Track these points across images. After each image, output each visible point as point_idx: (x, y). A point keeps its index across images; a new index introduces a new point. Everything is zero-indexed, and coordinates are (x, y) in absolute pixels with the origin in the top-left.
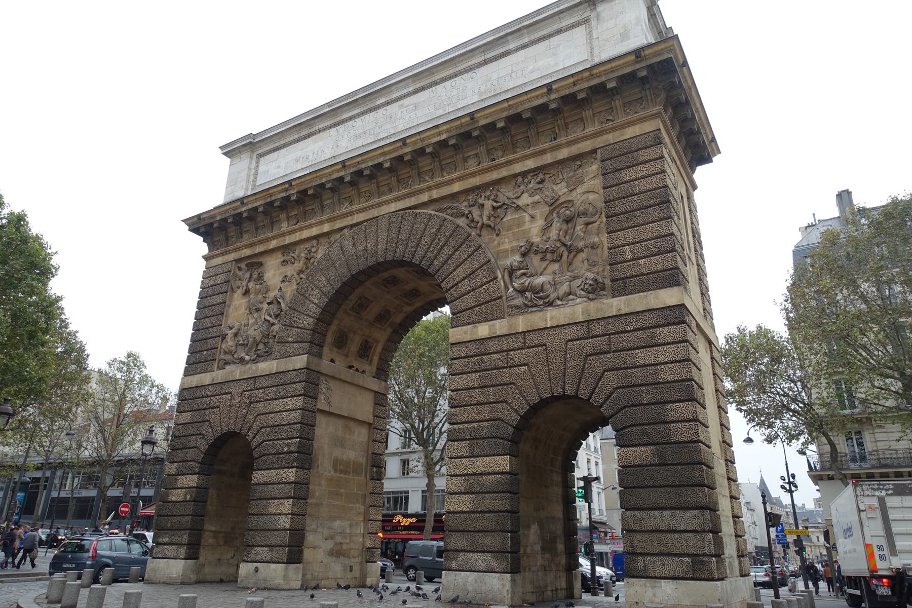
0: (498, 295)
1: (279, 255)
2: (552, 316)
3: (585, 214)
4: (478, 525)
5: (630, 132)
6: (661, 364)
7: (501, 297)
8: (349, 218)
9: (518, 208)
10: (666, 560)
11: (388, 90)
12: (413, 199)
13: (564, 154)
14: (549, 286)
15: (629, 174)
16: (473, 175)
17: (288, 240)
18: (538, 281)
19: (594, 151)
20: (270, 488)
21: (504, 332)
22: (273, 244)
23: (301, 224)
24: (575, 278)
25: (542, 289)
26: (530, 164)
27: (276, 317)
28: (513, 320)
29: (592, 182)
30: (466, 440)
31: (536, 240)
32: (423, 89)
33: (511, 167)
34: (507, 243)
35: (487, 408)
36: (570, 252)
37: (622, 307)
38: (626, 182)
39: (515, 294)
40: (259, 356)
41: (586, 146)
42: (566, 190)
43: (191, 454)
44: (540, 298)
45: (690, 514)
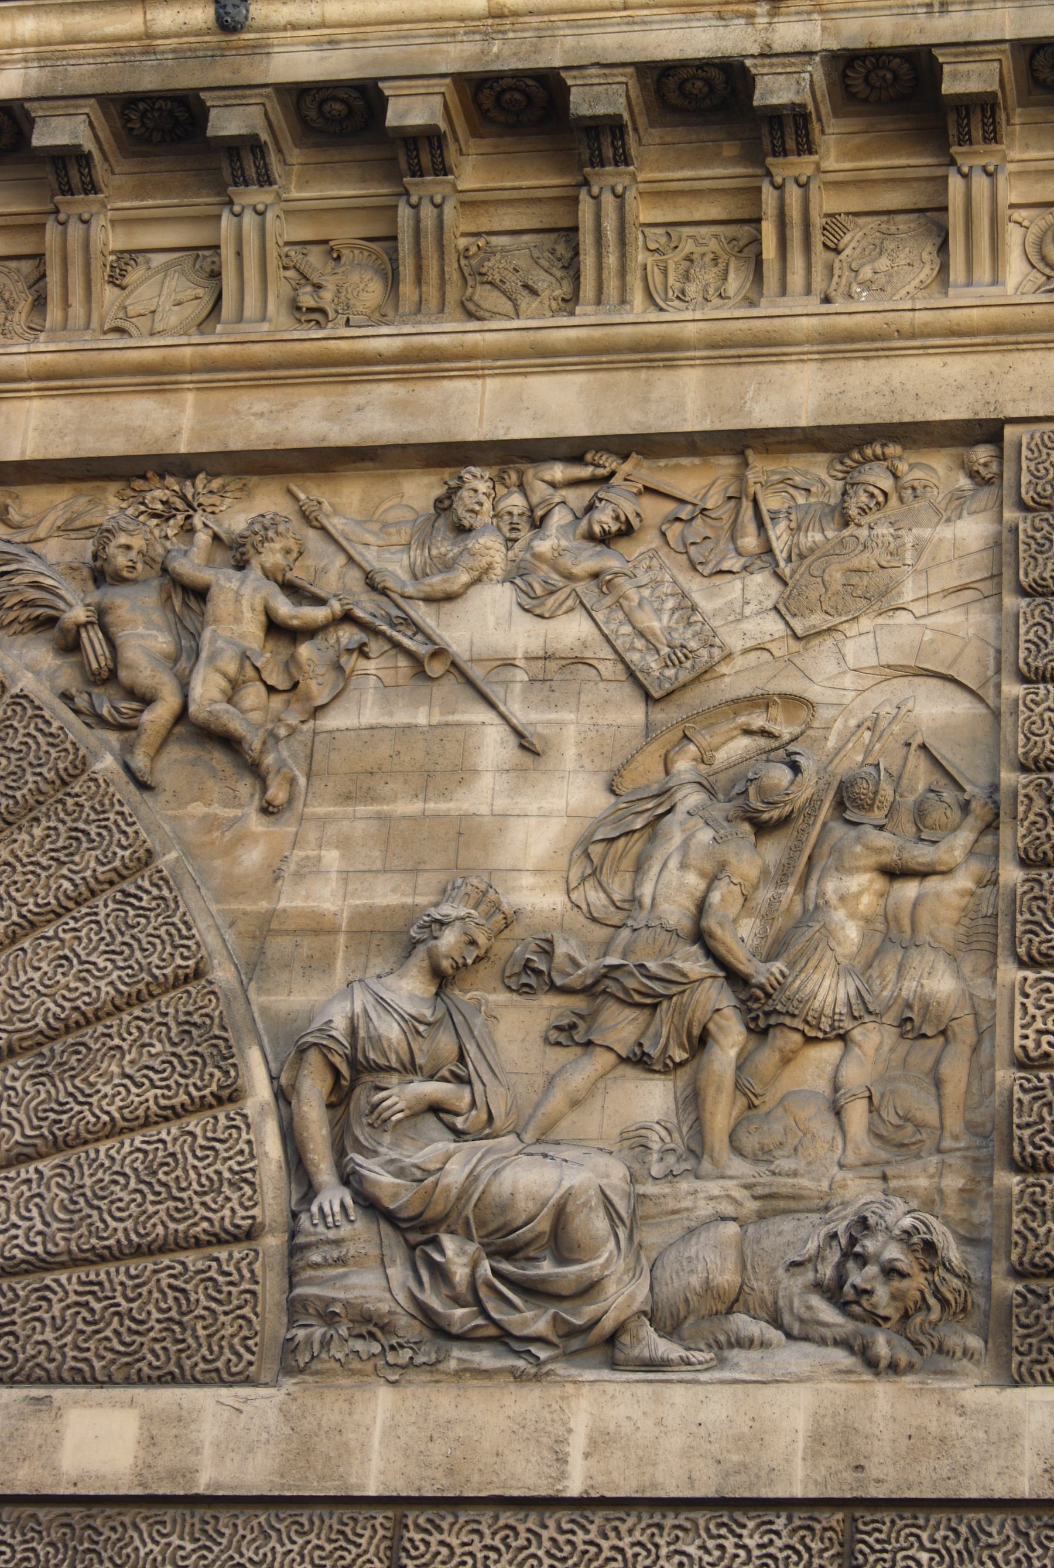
0: (230, 1213)
7: (250, 1235)
13: (794, 394)
14: (600, 1224)
16: (158, 378)
18: (528, 1181)
19: (989, 431)
21: (255, 1475)
24: (774, 1204)
25: (560, 1239)
26: (561, 405)
28: (327, 1407)
33: (429, 393)
39: (359, 1233)
42: (773, 626)
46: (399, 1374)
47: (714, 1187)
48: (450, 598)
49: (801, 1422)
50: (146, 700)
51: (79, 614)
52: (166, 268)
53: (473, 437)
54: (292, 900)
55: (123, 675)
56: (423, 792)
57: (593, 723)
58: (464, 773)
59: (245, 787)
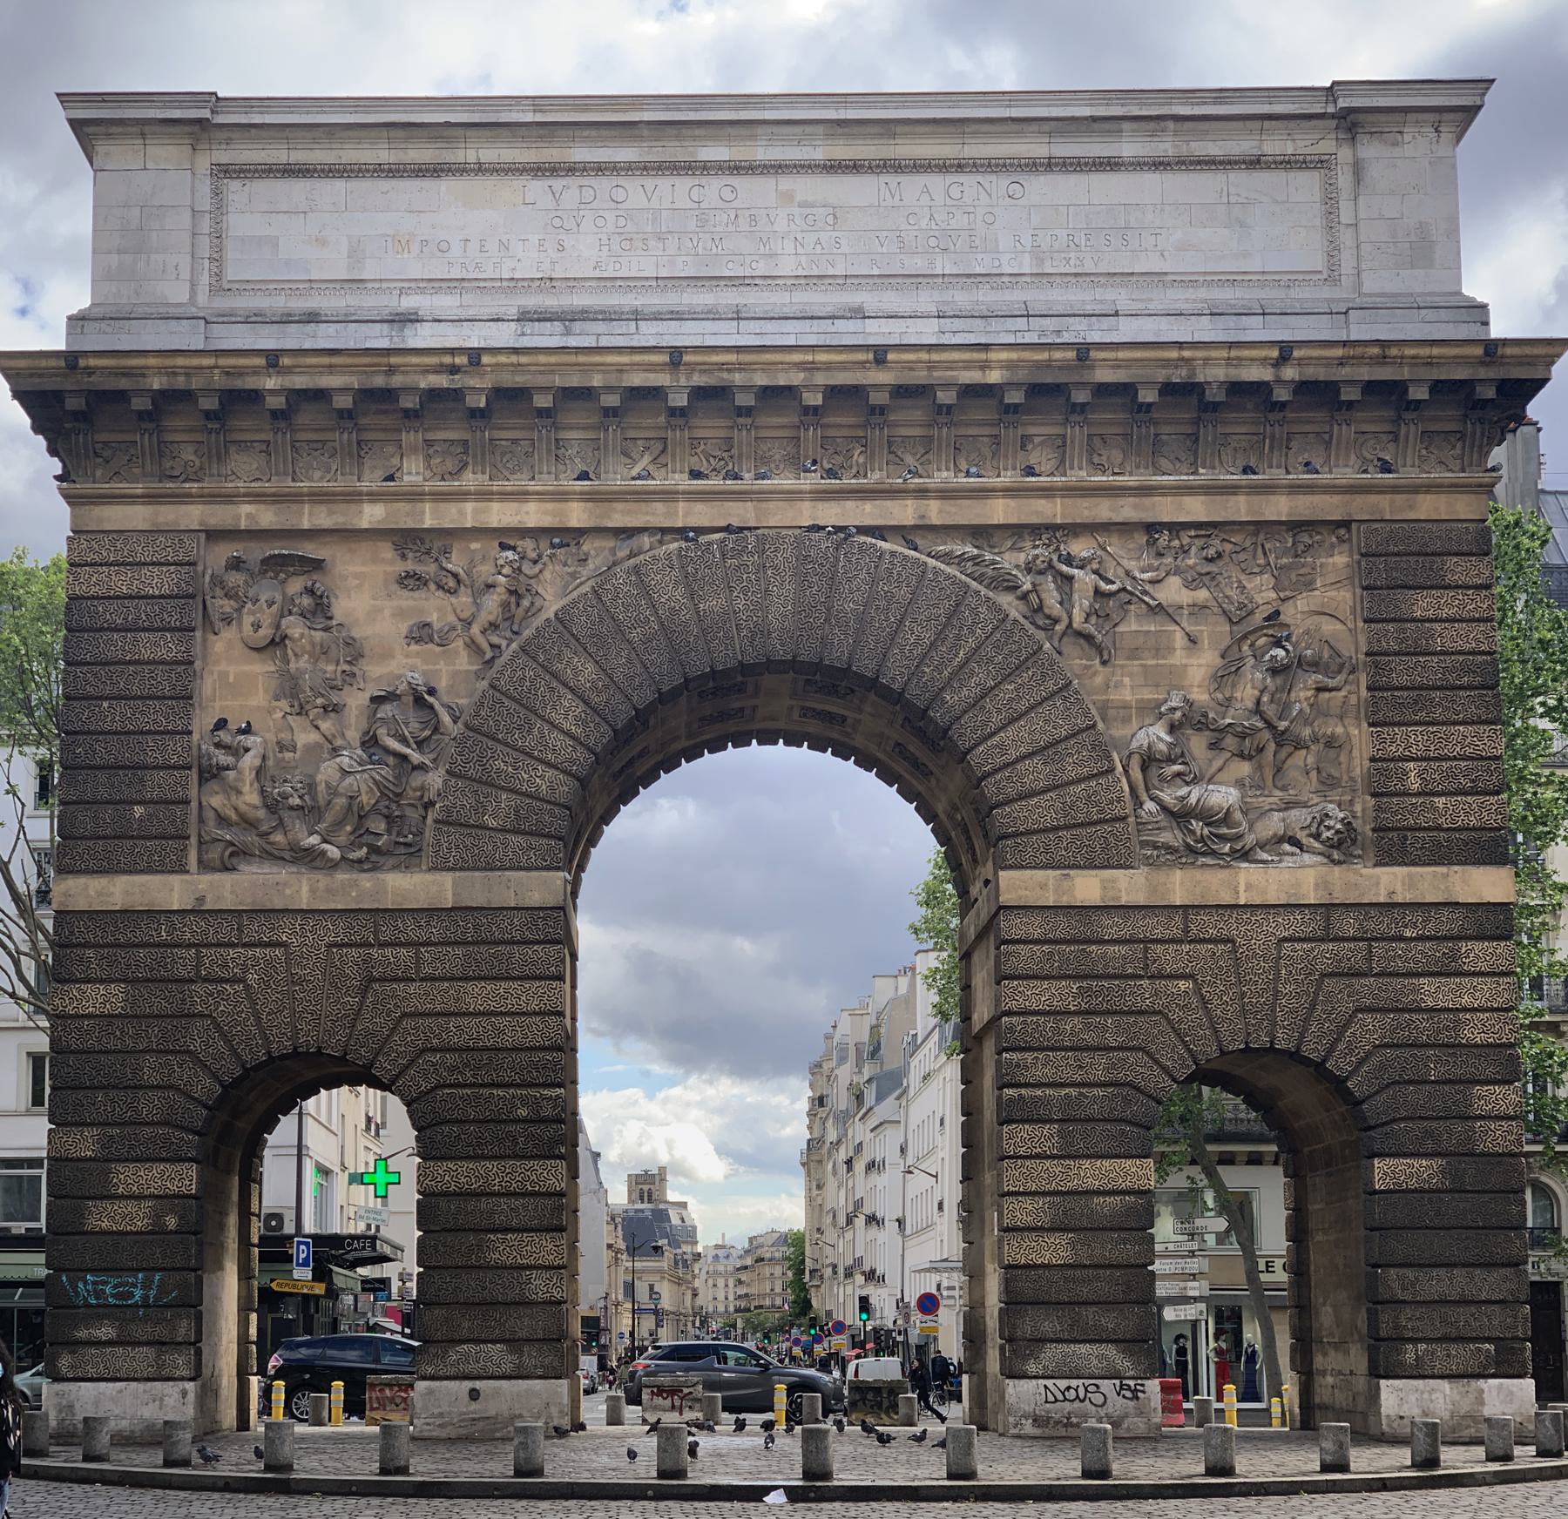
0: (1117, 811)
1: (387, 551)
2: (1253, 882)
3: (1315, 665)
4: (1085, 1292)
5: (1427, 507)
6: (1465, 1010)
8: (659, 506)
9: (1158, 610)
10: (1454, 1349)
11: (743, 131)
12: (868, 506)
13: (1279, 508)
15: (1422, 604)
16: (1047, 492)
17: (429, 517)
19: (1346, 524)
20: (484, 1204)
22: (372, 515)
23: (471, 480)
26: (1196, 509)
27: (420, 744)
28: (1161, 876)
29: (1333, 594)
30: (1052, 1121)
31: (1200, 697)
32: (854, 167)
33: (1147, 501)
34: (1126, 688)
35: (1102, 1059)
36: (1279, 745)
37: (1399, 888)
38: (1414, 620)
40: (374, 850)
41: (1329, 507)
42: (1274, 595)
43: (149, 1106)
44: (1223, 838)
45: (1496, 1275)
46: (1183, 866)
47: (1271, 800)
48: (1159, 582)
49: (1312, 880)
50: (1056, 621)
51: (1027, 586)
52: (1042, 443)
53: (1166, 520)
54: (1113, 696)
55: (1047, 611)
56: (1156, 657)
57: (1215, 633)
58: (1171, 650)
59: (1093, 652)
